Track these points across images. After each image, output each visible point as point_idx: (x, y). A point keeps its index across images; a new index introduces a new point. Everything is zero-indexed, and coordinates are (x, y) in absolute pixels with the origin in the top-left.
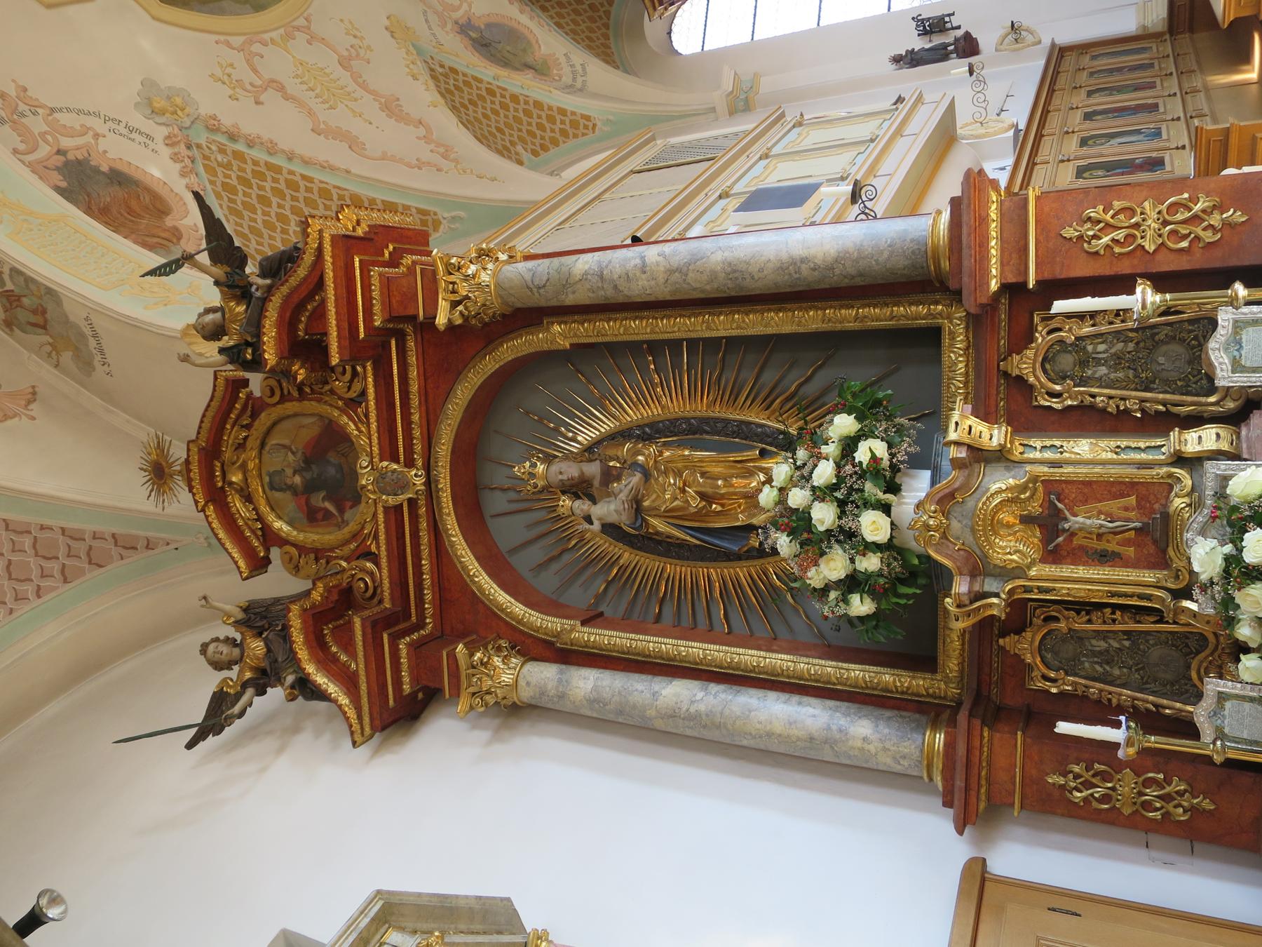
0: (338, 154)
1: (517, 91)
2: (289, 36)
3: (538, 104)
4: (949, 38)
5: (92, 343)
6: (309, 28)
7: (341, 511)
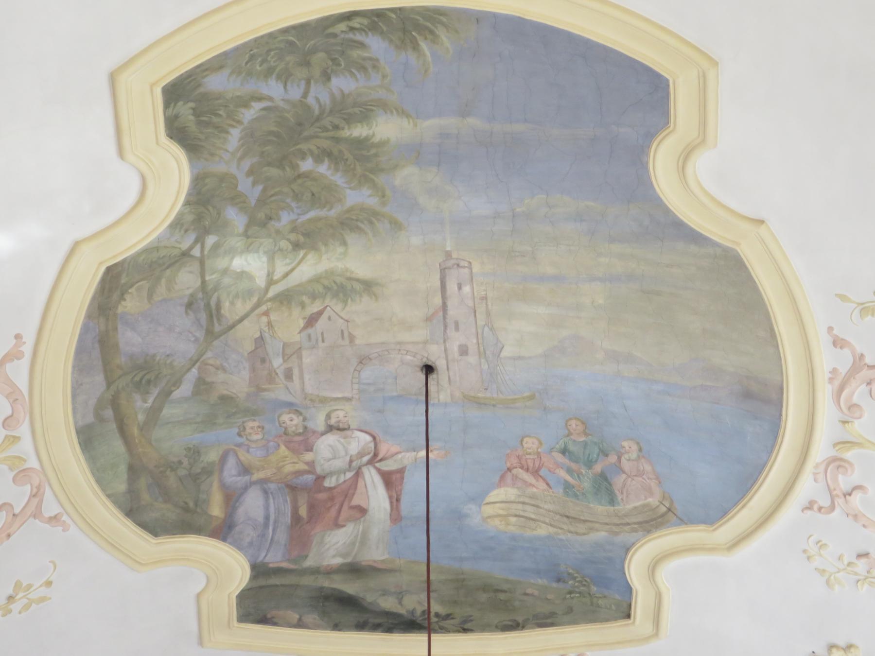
2: (22, 475)
6: (37, 514)
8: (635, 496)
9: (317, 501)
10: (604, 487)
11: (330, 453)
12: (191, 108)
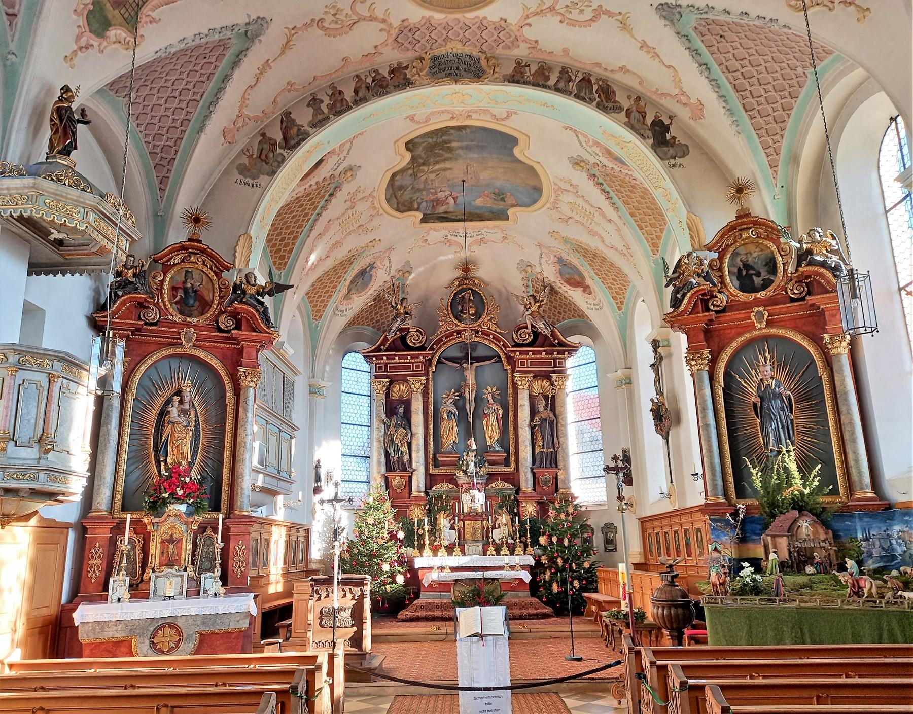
1: (338, 288)
3: (331, 296)
4: (322, 483)
5: (251, 181)
7: (176, 303)
8: (510, 201)
9: (437, 202)
10: (503, 200)
11: (440, 195)
12: (410, 145)
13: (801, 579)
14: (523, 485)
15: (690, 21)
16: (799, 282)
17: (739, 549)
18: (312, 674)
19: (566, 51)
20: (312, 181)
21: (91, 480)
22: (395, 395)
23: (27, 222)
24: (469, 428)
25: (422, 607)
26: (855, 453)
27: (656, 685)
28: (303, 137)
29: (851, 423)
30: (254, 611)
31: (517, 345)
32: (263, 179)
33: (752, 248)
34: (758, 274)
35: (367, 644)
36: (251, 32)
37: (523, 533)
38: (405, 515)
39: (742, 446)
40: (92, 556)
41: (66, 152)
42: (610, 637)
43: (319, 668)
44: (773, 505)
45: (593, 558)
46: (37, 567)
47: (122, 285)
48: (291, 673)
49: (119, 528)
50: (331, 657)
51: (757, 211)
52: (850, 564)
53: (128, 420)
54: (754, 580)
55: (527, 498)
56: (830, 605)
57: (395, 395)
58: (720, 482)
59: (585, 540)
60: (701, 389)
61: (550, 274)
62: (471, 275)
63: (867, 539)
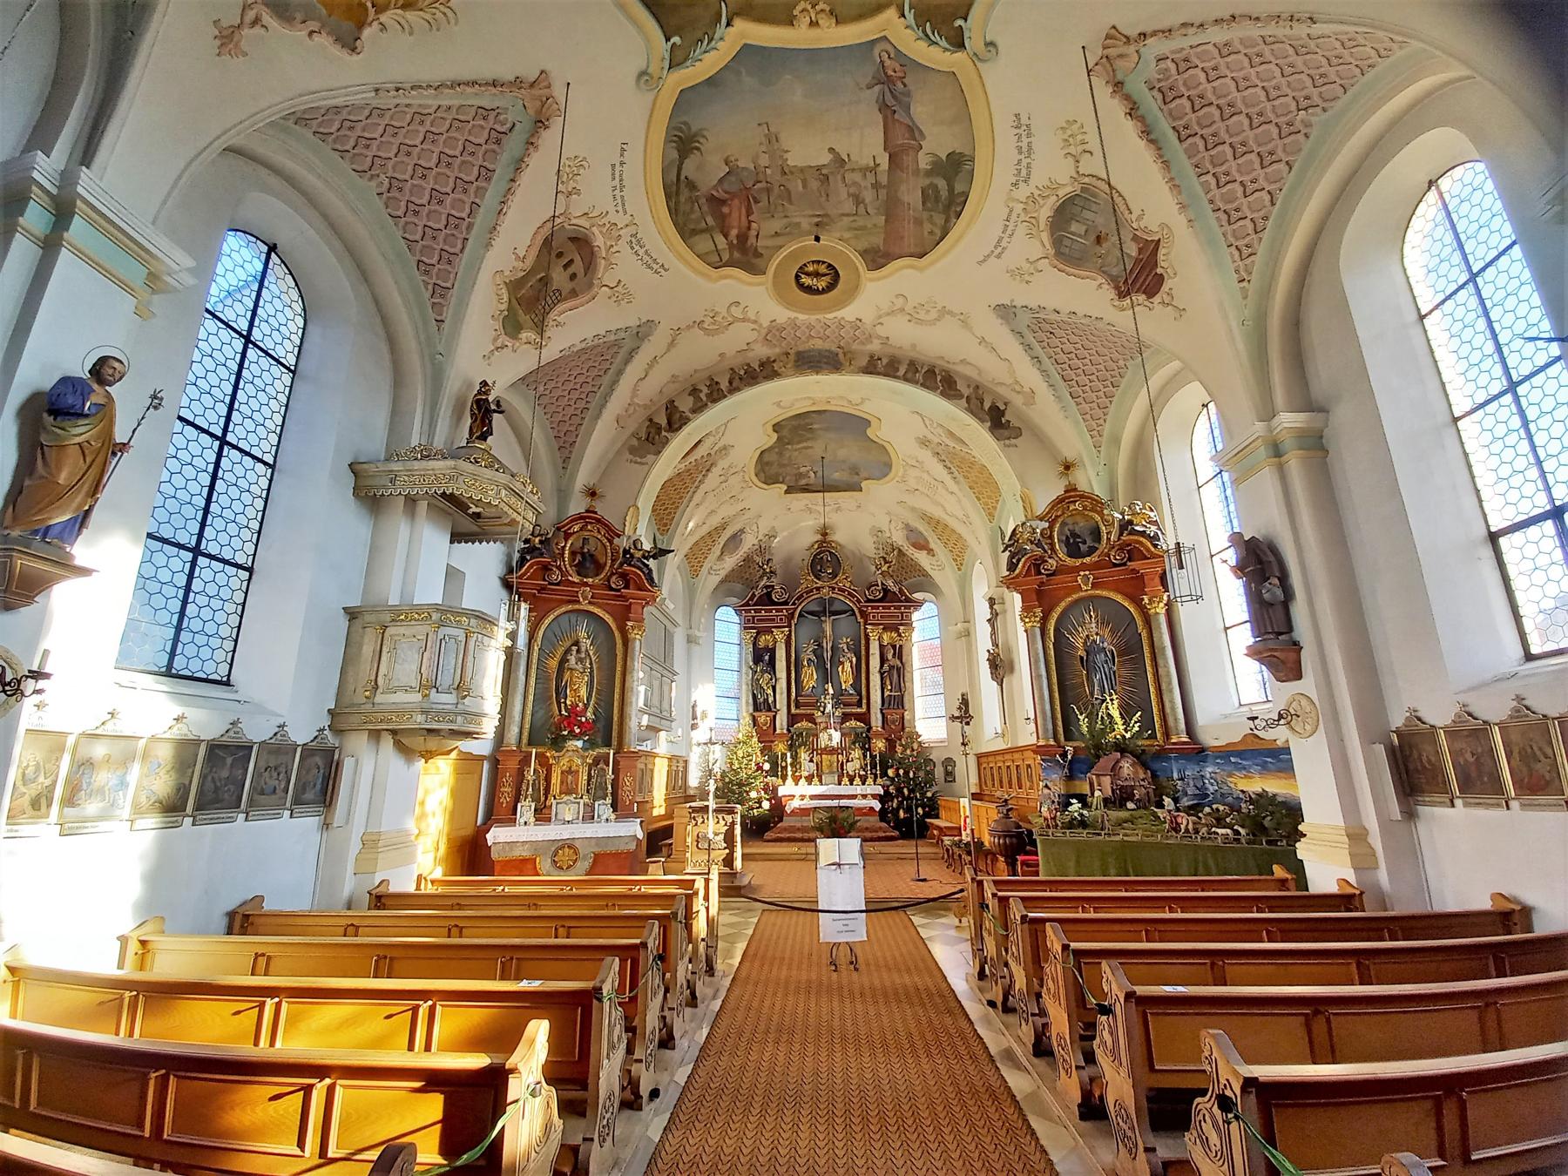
0: (697, 498)
4: (698, 721)
8: (864, 474)
9: (801, 476)
11: (803, 470)
12: (777, 427)
13: (1123, 814)
14: (873, 724)
15: (1024, 319)
16: (1121, 549)
17: (1067, 786)
18: (689, 899)
19: (914, 346)
20: (691, 459)
21: (502, 721)
22: (761, 644)
23: (451, 498)
24: (826, 675)
25: (785, 829)
26: (1172, 702)
27: (997, 913)
28: (685, 421)
29: (1168, 674)
30: (640, 835)
31: (869, 601)
32: (650, 458)
33: (1078, 518)
34: (1084, 542)
35: (738, 864)
36: (642, 332)
37: (874, 766)
38: (770, 749)
39: (1070, 694)
40: (504, 784)
41: (483, 437)
42: (951, 860)
43: (696, 893)
44: (1098, 747)
45: (935, 789)
46: (456, 794)
47: (529, 551)
48: (673, 896)
49: (526, 761)
50: (707, 881)
51: (1083, 486)
52: (1167, 801)
53: (534, 667)
54: (1081, 815)
55: (878, 735)
56: (1150, 839)
57: (761, 644)
58: (1050, 727)
59: (928, 773)
60: (1034, 642)
61: (899, 538)
62: (829, 538)
63: (1182, 779)
